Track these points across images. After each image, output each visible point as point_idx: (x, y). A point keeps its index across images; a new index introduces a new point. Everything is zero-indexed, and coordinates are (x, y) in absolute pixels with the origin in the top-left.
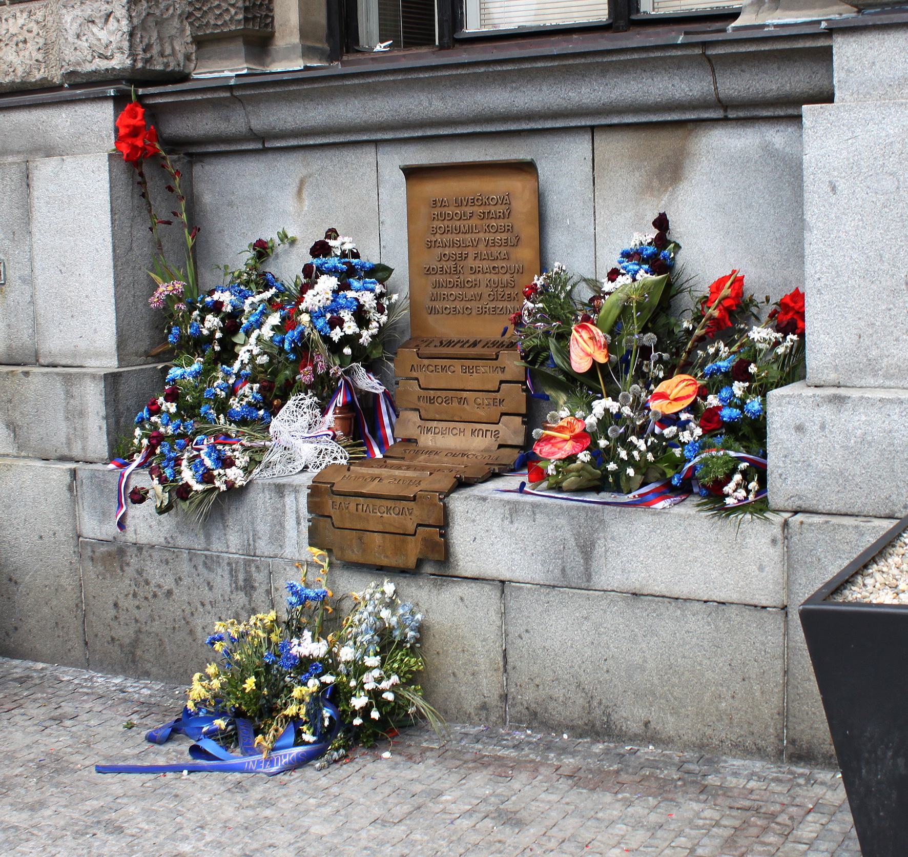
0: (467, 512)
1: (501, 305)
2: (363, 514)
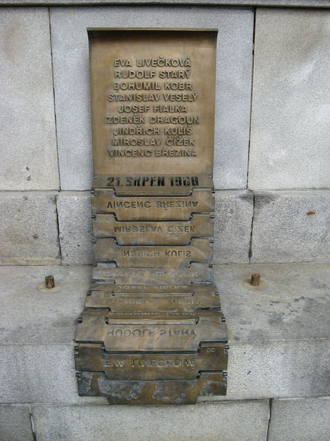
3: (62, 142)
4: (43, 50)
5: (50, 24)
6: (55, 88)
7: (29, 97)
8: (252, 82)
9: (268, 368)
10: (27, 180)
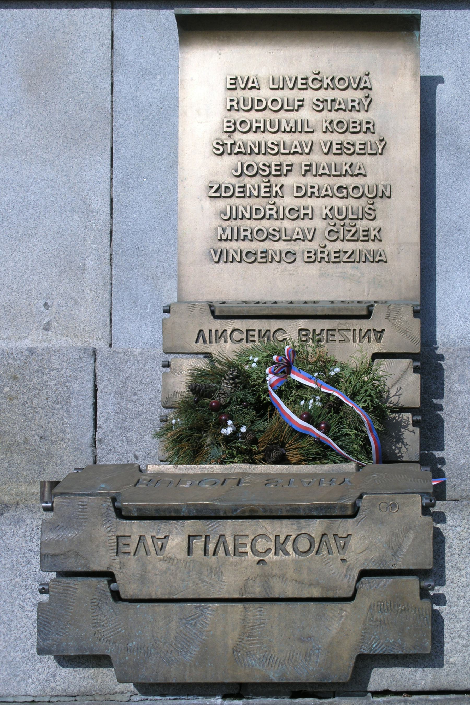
1: (349, 247)
3: (123, 251)
4: (97, 76)
6: (114, 147)
10: (44, 329)
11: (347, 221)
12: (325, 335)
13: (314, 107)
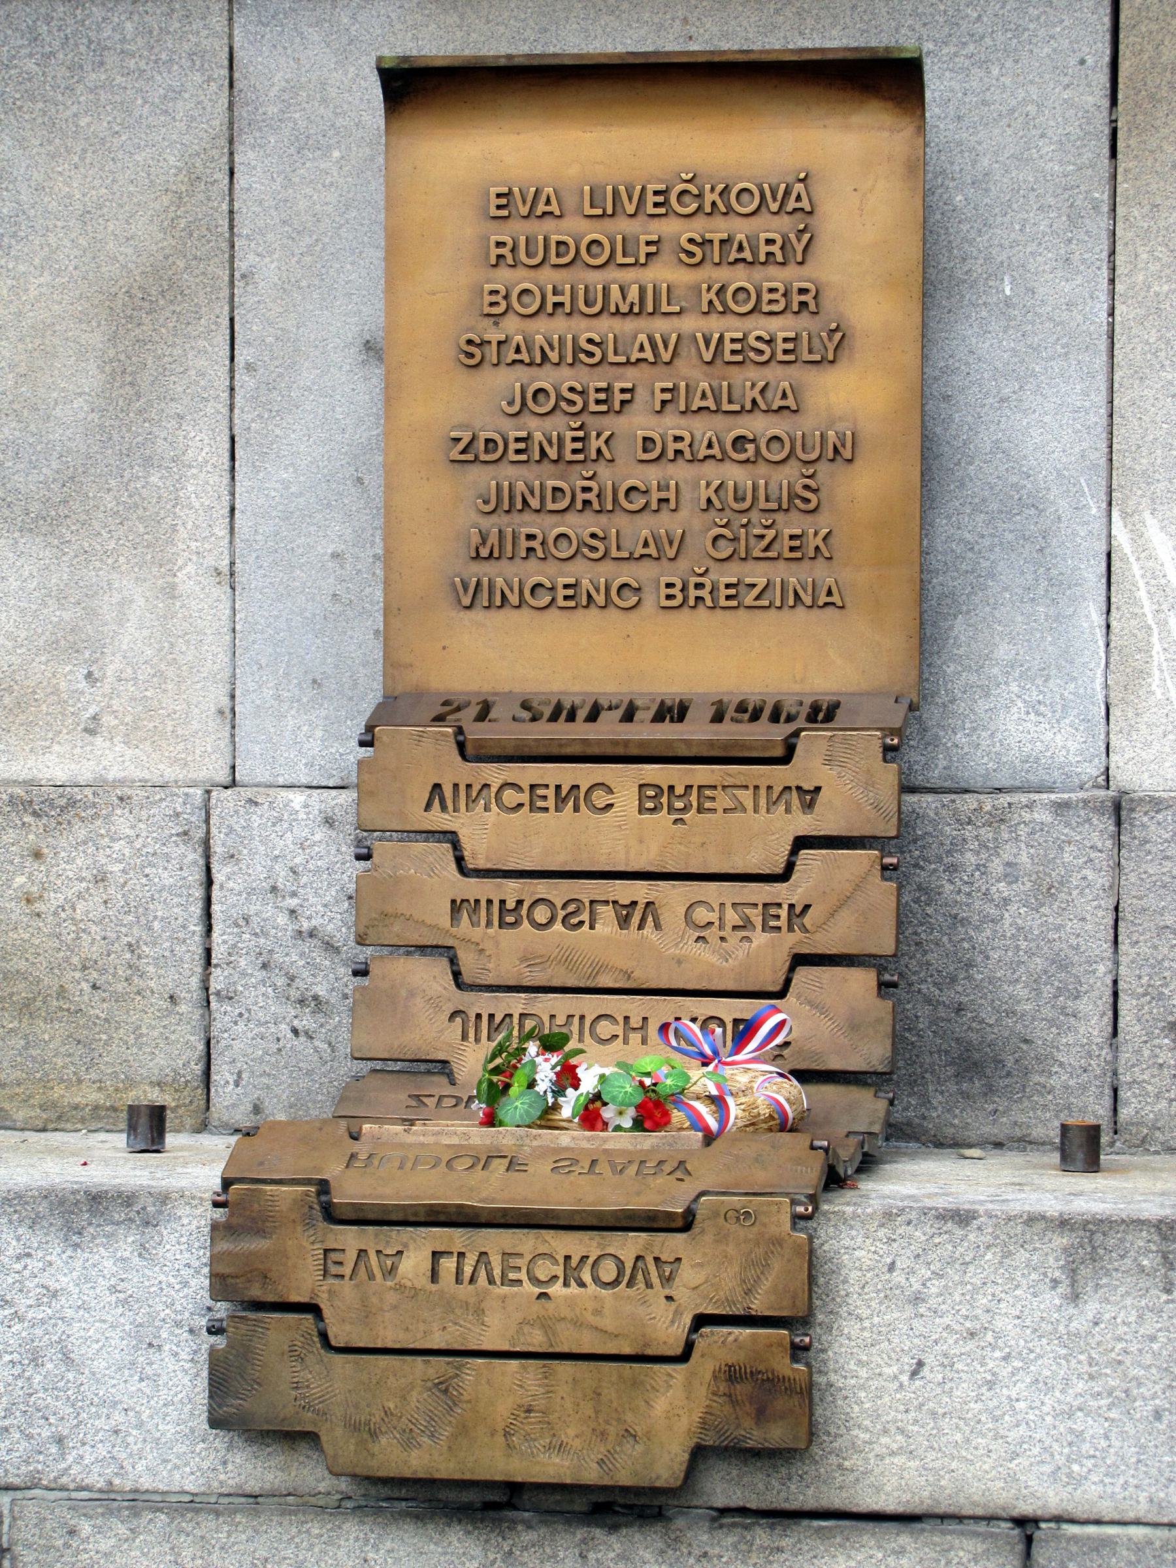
0: (892, 1267)
1: (758, 574)
2: (465, 1290)
3: (257, 557)
5: (231, 49)
6: (237, 319)
7: (122, 357)
8: (1112, 281)
9: (998, 1354)
10: (86, 730)
11: (755, 515)
12: (694, 799)
13: (683, 256)
